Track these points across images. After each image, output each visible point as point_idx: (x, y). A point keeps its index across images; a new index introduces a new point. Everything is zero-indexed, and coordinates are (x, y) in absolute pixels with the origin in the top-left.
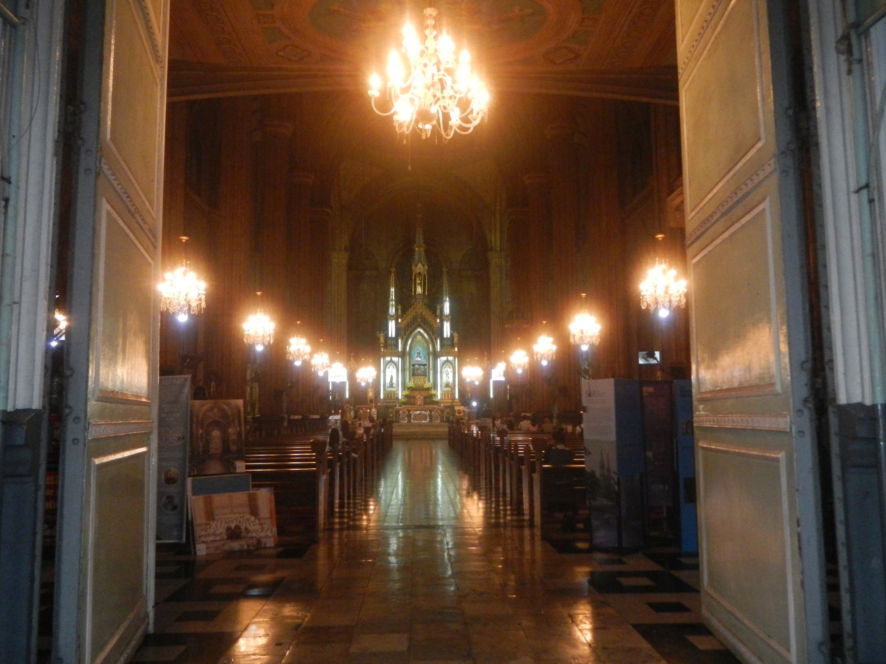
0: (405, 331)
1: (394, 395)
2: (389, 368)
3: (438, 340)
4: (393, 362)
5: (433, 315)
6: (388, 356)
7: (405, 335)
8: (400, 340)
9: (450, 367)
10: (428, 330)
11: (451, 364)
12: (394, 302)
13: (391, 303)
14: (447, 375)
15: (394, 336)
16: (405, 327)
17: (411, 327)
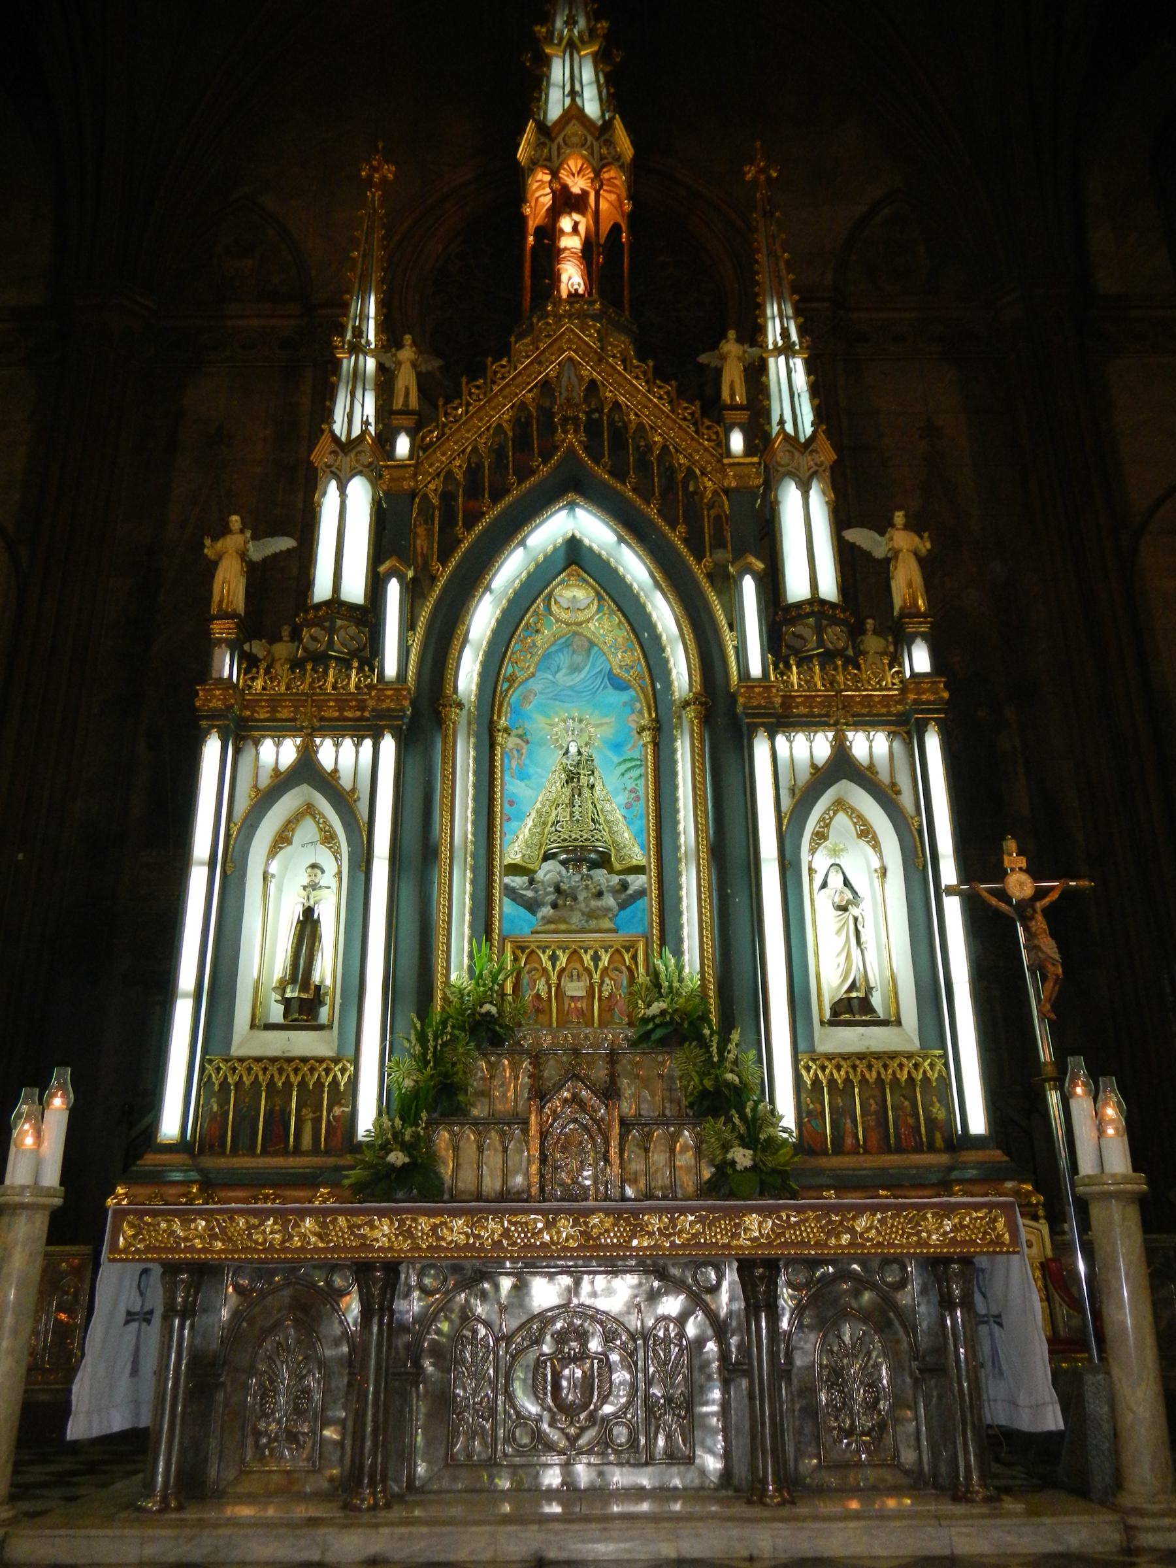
0: (448, 521)
1: (310, 1097)
2: (282, 840)
3: (749, 586)
4: (327, 783)
5: (696, 408)
6: (280, 731)
7: (444, 559)
8: (393, 589)
9: (866, 833)
10: (652, 512)
11: (886, 797)
12: (371, 364)
13: (348, 363)
14: (843, 909)
15: (355, 590)
16: (447, 497)
17: (496, 498)
